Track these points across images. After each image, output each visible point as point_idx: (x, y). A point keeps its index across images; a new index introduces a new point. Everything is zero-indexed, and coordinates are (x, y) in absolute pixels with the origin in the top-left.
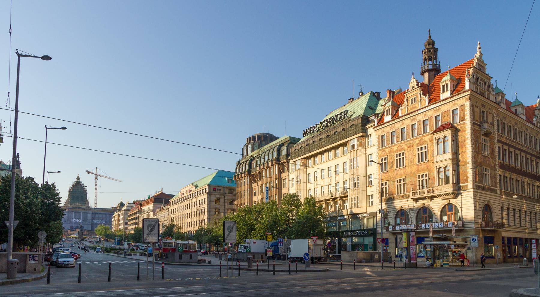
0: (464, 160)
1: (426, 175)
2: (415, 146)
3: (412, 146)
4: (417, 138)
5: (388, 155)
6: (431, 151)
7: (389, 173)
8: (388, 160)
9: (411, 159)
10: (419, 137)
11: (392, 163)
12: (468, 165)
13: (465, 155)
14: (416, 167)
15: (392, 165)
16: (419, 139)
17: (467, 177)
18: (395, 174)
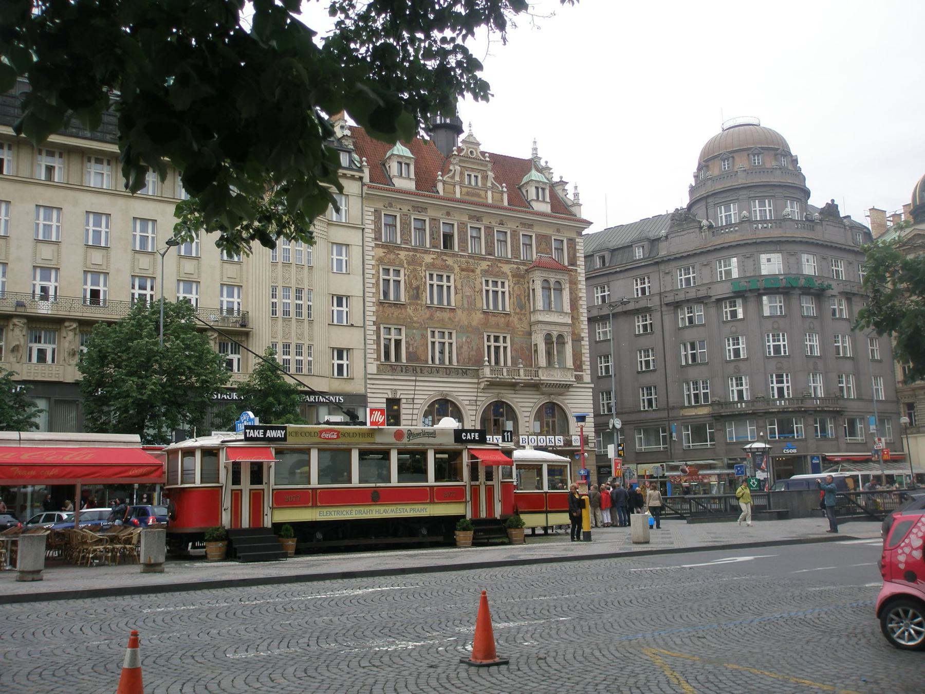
0: (576, 332)
1: (505, 338)
2: (478, 271)
3: (473, 271)
4: (485, 259)
5: (406, 265)
6: (515, 296)
7: (408, 310)
8: (406, 277)
9: (468, 297)
10: (489, 260)
11: (418, 288)
12: (583, 343)
13: (577, 324)
14: (482, 316)
15: (418, 293)
16: (489, 263)
17: (581, 362)
18: (428, 315)
